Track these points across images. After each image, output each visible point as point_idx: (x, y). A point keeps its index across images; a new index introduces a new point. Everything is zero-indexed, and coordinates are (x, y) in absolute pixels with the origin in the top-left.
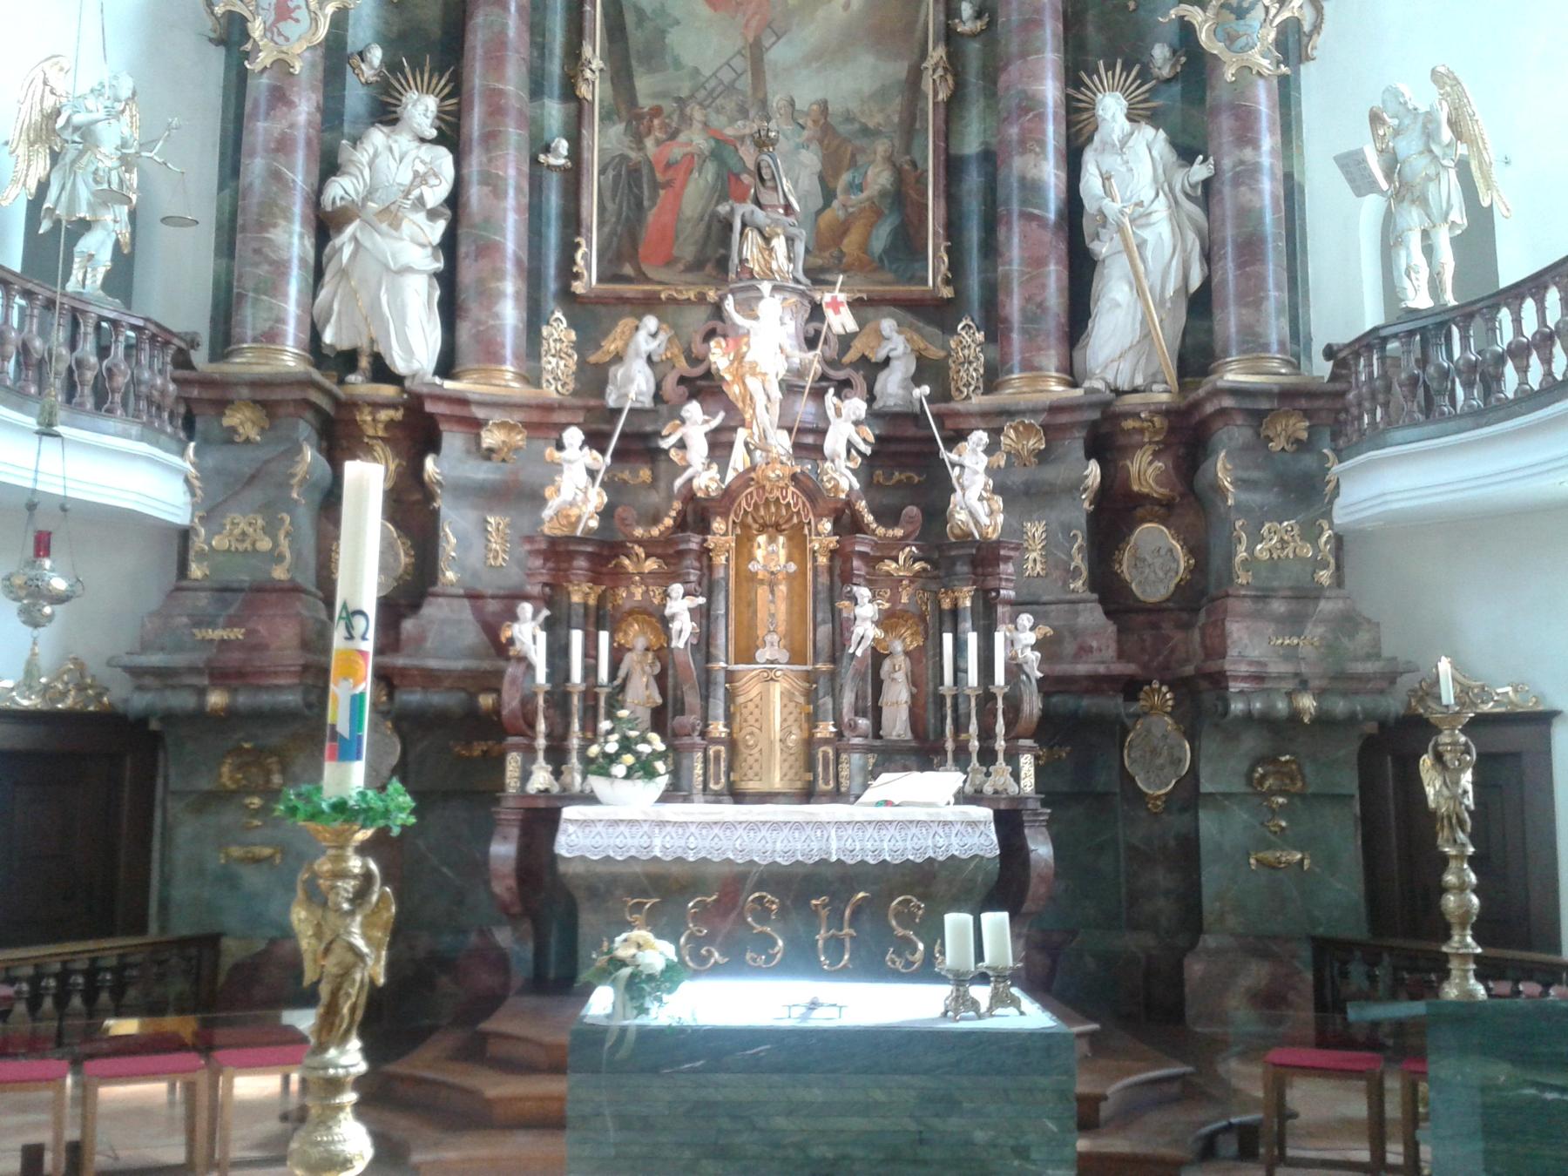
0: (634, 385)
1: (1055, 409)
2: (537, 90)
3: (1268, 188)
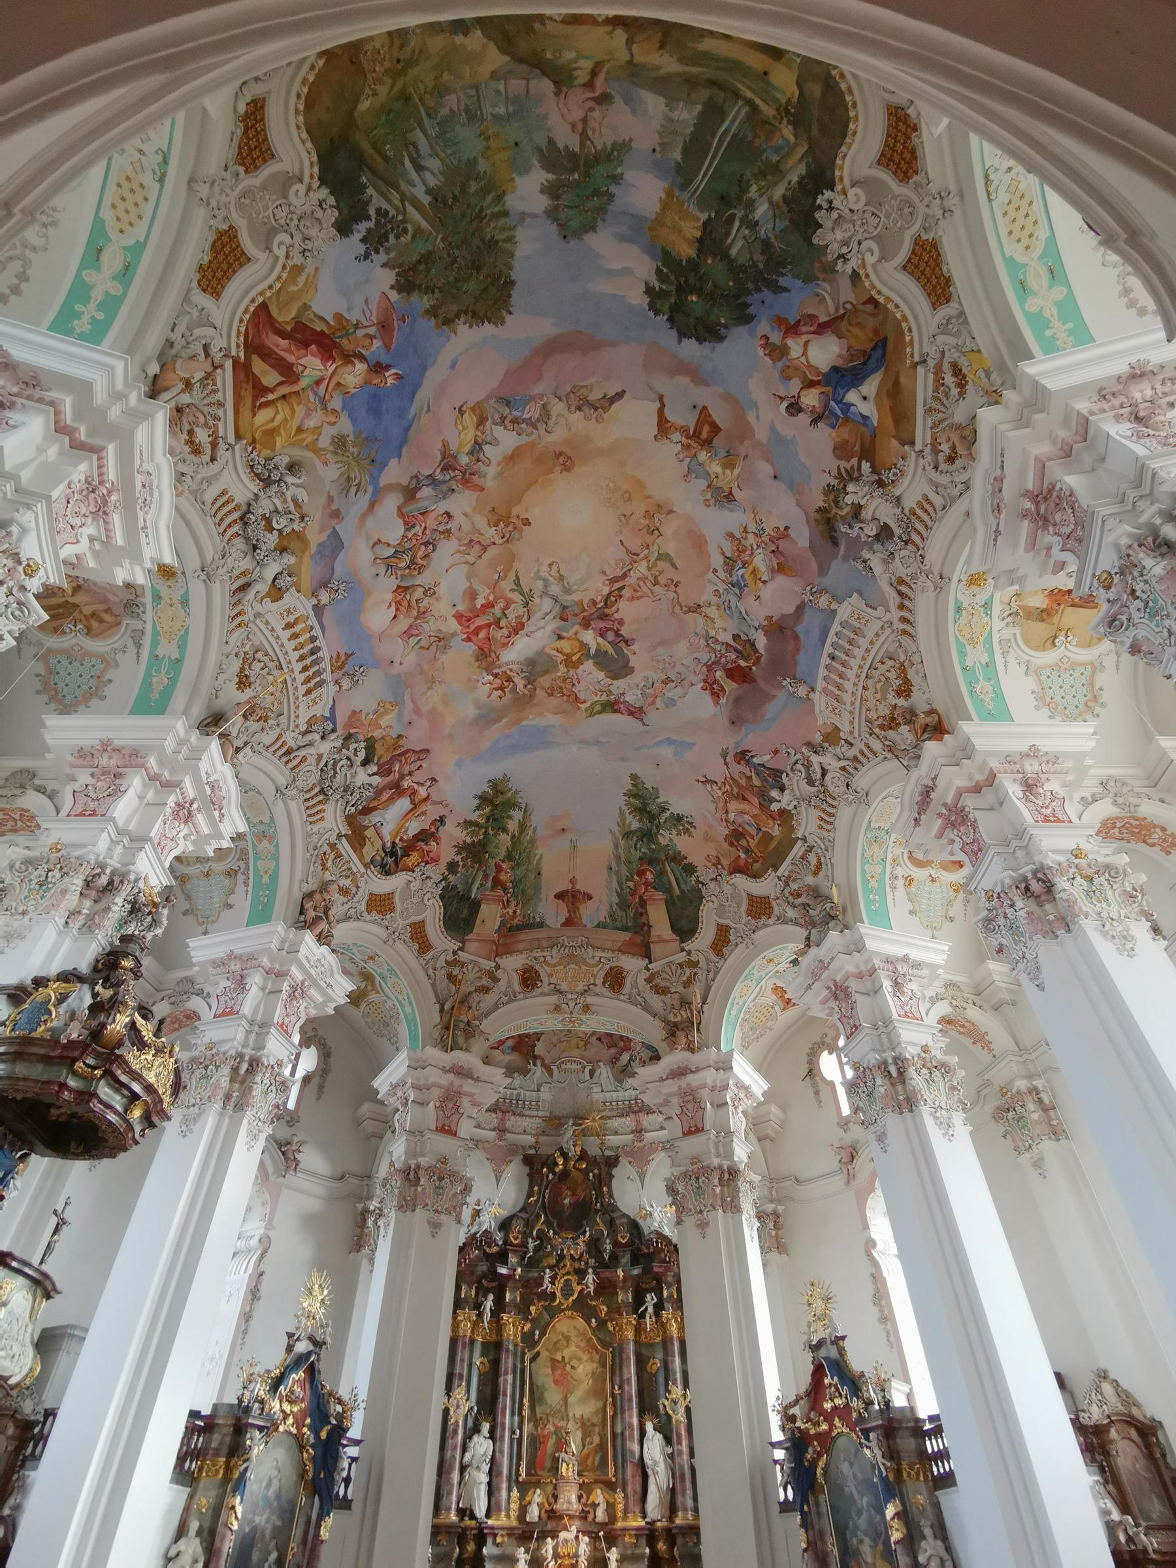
0: (534, 1514)
1: (638, 1529)
2: (513, 1414)
3: (685, 1457)
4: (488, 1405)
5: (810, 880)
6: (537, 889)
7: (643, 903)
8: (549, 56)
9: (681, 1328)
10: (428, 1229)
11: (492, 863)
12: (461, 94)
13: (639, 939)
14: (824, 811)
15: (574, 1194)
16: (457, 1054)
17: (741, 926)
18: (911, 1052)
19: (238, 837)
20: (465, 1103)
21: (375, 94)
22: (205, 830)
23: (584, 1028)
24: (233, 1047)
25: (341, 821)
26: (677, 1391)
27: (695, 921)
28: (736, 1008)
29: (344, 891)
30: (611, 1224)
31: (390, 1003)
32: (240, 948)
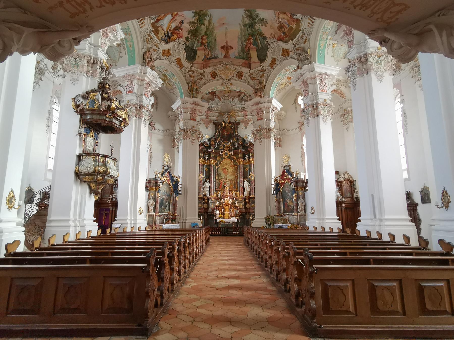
0: (219, 195)
4: (208, 176)
5: (302, 45)
6: (215, 45)
7: (249, 50)
9: (254, 162)
10: (191, 143)
11: (200, 37)
13: (247, 62)
14: (311, 20)
15: (227, 132)
16: (194, 99)
17: (279, 59)
18: (320, 101)
19: (122, 40)
20: (198, 112)
22: (113, 39)
23: (230, 89)
24: (134, 102)
25: (150, 25)
26: (252, 174)
27: (265, 56)
28: (275, 84)
29: (155, 50)
30: (237, 139)
31: (172, 83)
32: (130, 72)
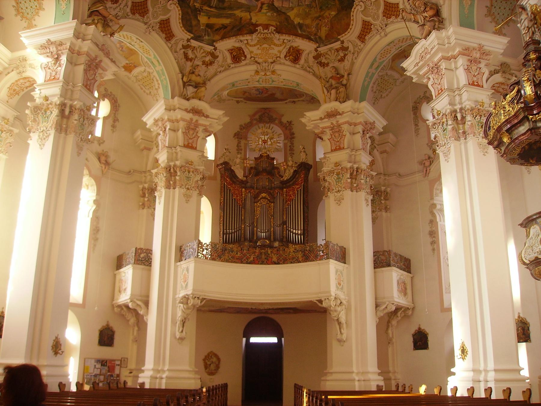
8: (275, 14)
12: (304, 3)
21: (330, 14)
